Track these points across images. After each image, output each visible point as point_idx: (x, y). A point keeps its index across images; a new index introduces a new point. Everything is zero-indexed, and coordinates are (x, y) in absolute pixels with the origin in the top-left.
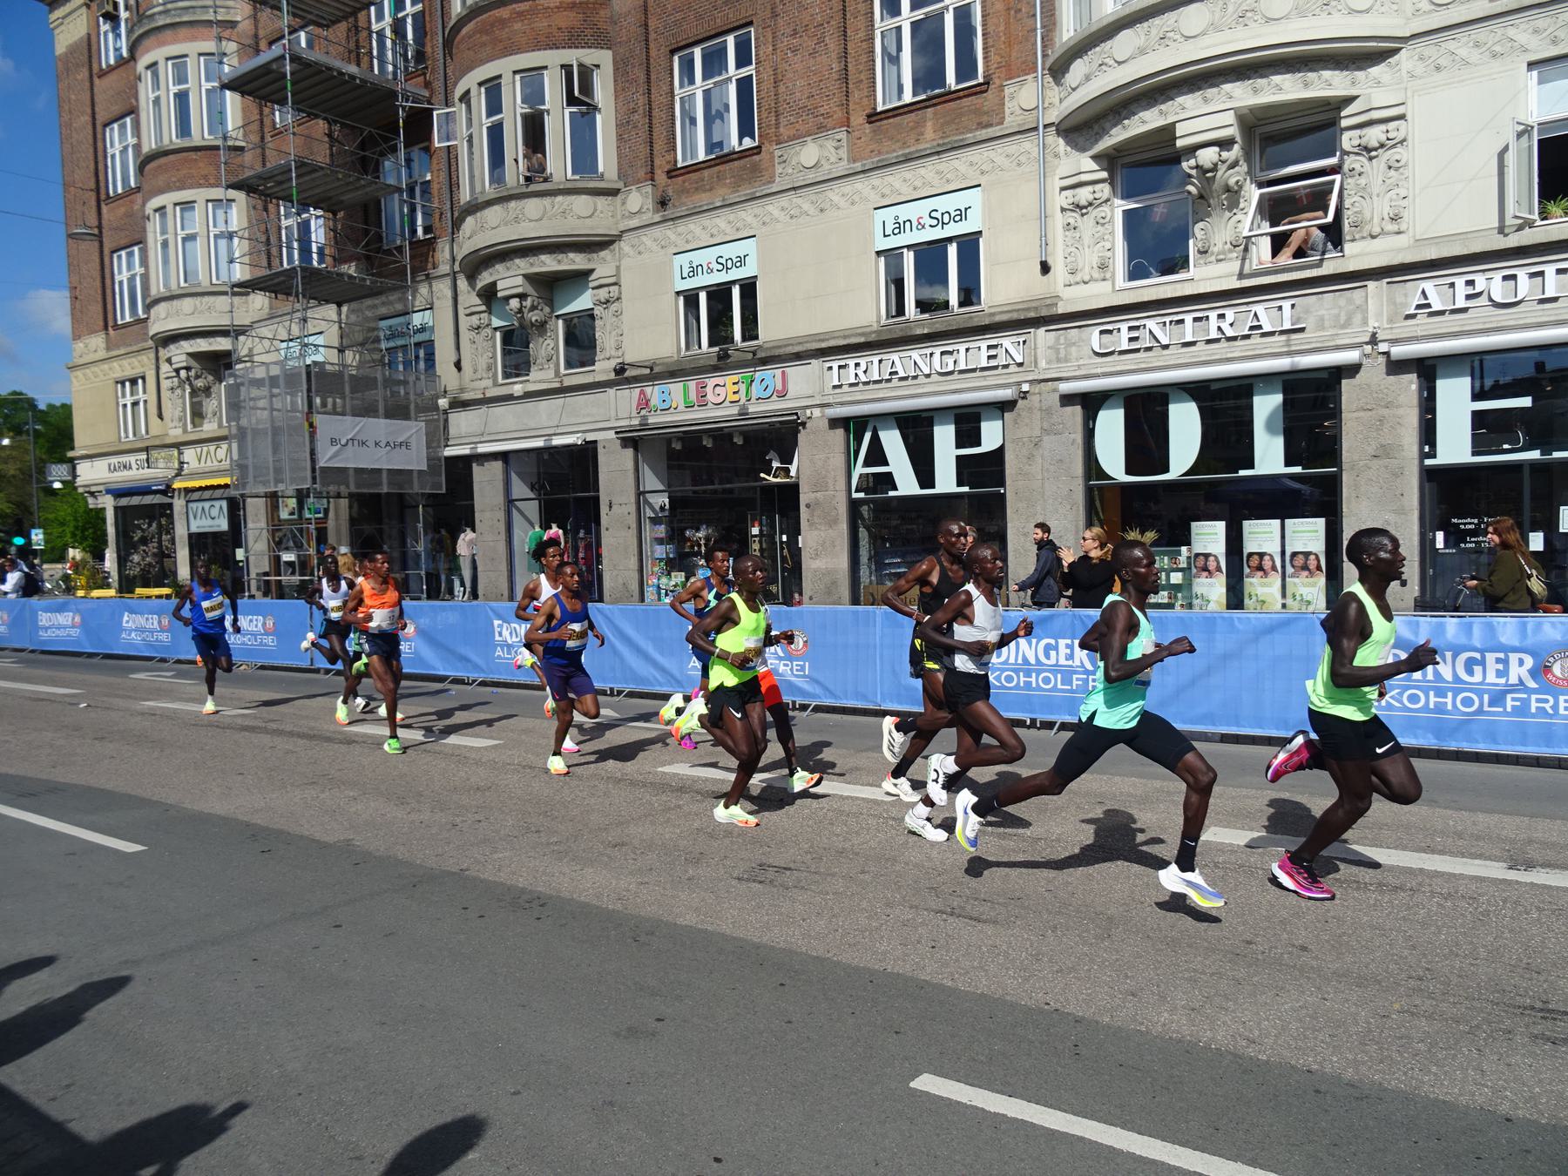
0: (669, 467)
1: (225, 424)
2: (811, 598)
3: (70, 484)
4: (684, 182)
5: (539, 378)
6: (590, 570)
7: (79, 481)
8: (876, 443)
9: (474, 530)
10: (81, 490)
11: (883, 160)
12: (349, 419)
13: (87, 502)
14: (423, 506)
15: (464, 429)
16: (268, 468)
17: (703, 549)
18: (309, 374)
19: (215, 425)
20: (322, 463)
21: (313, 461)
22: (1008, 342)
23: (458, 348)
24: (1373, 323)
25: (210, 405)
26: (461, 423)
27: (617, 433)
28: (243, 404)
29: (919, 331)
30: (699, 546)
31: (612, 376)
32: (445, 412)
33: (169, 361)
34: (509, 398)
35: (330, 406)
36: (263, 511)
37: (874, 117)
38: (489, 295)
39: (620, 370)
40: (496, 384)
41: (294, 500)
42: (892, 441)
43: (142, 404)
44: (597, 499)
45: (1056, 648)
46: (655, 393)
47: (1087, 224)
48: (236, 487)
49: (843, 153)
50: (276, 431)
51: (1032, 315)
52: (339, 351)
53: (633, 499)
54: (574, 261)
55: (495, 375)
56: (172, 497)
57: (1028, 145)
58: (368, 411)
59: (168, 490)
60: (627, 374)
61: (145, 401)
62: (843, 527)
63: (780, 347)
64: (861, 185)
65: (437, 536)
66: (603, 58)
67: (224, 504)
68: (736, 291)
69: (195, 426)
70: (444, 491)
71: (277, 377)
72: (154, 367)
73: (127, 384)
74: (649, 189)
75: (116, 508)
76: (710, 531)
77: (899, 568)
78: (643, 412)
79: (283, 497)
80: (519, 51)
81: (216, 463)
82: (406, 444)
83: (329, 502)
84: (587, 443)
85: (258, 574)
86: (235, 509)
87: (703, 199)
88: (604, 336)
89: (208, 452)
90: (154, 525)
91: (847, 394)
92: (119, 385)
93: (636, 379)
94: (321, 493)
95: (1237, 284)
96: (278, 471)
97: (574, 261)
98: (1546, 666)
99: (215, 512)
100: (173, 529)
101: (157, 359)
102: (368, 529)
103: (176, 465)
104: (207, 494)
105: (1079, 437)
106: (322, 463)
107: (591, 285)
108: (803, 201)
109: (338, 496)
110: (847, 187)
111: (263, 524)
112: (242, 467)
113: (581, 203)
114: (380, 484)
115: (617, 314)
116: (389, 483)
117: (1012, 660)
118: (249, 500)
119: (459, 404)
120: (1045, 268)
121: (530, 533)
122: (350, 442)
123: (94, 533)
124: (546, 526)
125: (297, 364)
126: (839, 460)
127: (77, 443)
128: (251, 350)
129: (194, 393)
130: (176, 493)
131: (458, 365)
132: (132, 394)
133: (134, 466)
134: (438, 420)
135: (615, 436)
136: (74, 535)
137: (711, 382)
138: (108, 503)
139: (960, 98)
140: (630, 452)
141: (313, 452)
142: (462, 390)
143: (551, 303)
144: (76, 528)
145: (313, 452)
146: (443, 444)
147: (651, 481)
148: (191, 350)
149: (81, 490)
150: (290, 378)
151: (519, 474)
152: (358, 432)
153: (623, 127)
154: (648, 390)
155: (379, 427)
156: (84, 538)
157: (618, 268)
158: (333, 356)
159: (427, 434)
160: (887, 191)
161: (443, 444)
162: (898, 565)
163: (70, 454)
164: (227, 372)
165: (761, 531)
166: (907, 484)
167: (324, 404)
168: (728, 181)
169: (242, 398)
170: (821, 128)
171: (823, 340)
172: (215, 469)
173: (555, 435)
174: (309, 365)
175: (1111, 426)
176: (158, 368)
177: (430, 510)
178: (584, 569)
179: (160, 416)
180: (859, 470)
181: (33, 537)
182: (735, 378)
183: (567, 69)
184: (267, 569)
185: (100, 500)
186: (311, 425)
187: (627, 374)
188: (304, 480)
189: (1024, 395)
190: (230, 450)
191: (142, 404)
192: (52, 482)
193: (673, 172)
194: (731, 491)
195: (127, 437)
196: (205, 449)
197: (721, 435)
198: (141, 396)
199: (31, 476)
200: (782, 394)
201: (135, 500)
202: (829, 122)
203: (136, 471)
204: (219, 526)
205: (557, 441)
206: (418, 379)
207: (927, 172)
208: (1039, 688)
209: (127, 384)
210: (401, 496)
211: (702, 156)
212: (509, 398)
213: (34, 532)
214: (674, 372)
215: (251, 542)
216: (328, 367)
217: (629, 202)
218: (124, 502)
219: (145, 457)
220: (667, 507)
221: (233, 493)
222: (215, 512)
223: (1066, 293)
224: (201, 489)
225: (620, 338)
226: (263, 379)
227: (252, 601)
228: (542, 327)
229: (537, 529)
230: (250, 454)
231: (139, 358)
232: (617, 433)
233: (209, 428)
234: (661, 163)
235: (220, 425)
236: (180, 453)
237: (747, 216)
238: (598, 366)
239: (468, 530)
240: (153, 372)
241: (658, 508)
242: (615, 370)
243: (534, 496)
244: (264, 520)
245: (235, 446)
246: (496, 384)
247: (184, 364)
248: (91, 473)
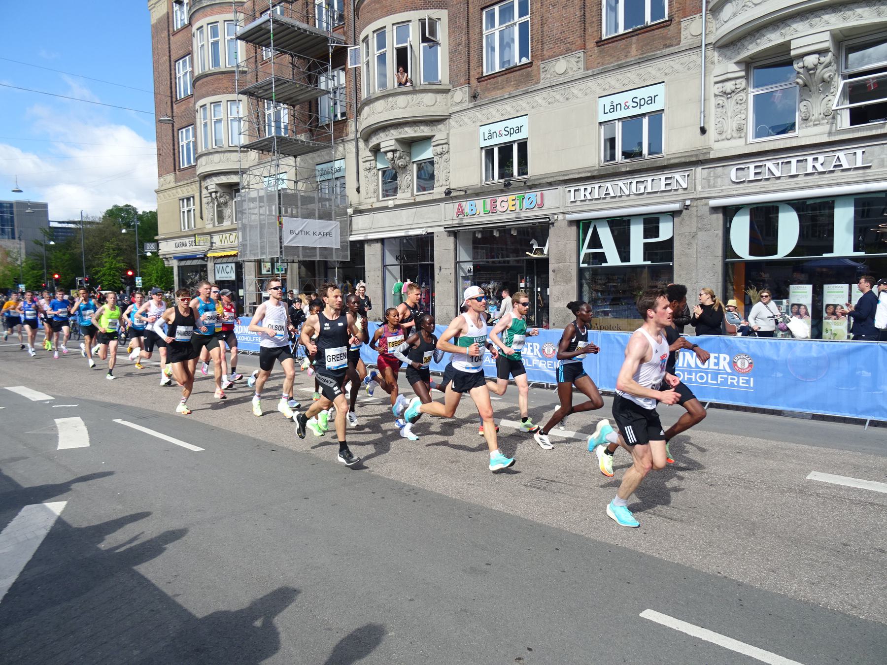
0: (474, 248)
1: (234, 222)
2: (554, 324)
3: (155, 254)
4: (487, 84)
5: (403, 197)
6: (428, 305)
7: (160, 252)
8: (595, 234)
9: (364, 282)
10: (161, 257)
11: (606, 68)
12: (300, 219)
13: (164, 263)
14: (338, 268)
15: (360, 227)
16: (257, 246)
17: (491, 294)
18: (279, 195)
19: (229, 223)
20: (285, 244)
21: (281, 242)
22: (678, 176)
23: (358, 181)
25: (227, 212)
26: (359, 222)
27: (445, 228)
28: (244, 212)
29: (623, 170)
30: (489, 293)
31: (443, 196)
32: (351, 216)
33: (207, 188)
34: (386, 208)
35: (289, 210)
36: (253, 269)
37: (600, 43)
38: (376, 150)
39: (448, 193)
40: (378, 201)
41: (270, 264)
42: (605, 235)
43: (192, 211)
44: (432, 266)
46: (467, 205)
47: (730, 105)
48: (241, 256)
49: (581, 65)
50: (262, 227)
51: (694, 159)
52: (295, 182)
53: (453, 266)
54: (424, 131)
55: (378, 196)
56: (207, 261)
57: (696, 58)
58: (309, 215)
59: (205, 258)
60: (453, 194)
61: (194, 210)
62: (574, 283)
63: (540, 179)
65: (345, 285)
66: (442, 15)
67: (233, 265)
69: (219, 224)
70: (349, 260)
71: (263, 196)
72: (199, 191)
73: (185, 200)
74: (467, 89)
75: (179, 267)
76: (496, 284)
77: (605, 308)
78: (460, 217)
79: (263, 262)
80: (396, 12)
81: (229, 243)
82: (329, 234)
83: (288, 265)
84: (428, 233)
85: (250, 304)
86: (239, 267)
87: (498, 94)
88: (440, 173)
89: (226, 237)
90: (198, 276)
91: (579, 206)
92: (181, 201)
93: (456, 197)
94: (284, 260)
95: (826, 139)
96: (262, 248)
97: (424, 131)
99: (228, 270)
100: (207, 278)
101: (200, 187)
102: (309, 280)
103: (209, 244)
104: (225, 260)
105: (720, 232)
106: (285, 244)
107: (433, 144)
108: (557, 94)
109: (293, 262)
110: (583, 85)
111: (253, 277)
112: (244, 246)
113: (428, 98)
114: (316, 256)
115: (447, 161)
116: (320, 255)
118: (246, 263)
119: (358, 212)
120: (703, 131)
121: (395, 284)
122: (300, 233)
123: (167, 279)
124: (404, 281)
125: (273, 190)
126: (573, 245)
127: (159, 233)
128: (249, 182)
129: (219, 206)
130: (209, 259)
131: (358, 190)
132: (187, 206)
133: (188, 245)
134: (347, 220)
135: (444, 230)
136: (156, 281)
137: (499, 200)
138: (175, 264)
139: (653, 30)
140: (452, 239)
141: (281, 238)
142: (360, 204)
143: (410, 154)
144: (158, 277)
145: (281, 238)
146: (349, 234)
147: (464, 256)
148: (218, 182)
149: (161, 257)
150: (270, 197)
151: (389, 251)
152: (304, 227)
153: (453, 54)
154: (463, 204)
155: (315, 224)
156: (162, 282)
157: (448, 134)
158: (292, 185)
159: (341, 228)
160: (607, 87)
161: (349, 234)
162: (605, 306)
163: (156, 238)
164: (237, 194)
165: (526, 285)
166: (613, 259)
167: (286, 212)
168: (512, 83)
169: (244, 208)
170: (568, 51)
171: (566, 175)
172: (229, 246)
173: (411, 229)
174: (280, 190)
175: (741, 228)
176: (201, 192)
177: (341, 270)
178: (424, 304)
179: (202, 218)
180: (585, 250)
181: (137, 281)
182: (513, 197)
183: (423, 21)
184: (255, 301)
185: (171, 262)
186: (280, 223)
187: (452, 195)
188: (276, 253)
189: (687, 207)
190: (237, 237)
191: (192, 211)
192: (146, 252)
193: (481, 79)
194: (508, 262)
195: (185, 229)
196: (224, 235)
197: (504, 230)
198: (192, 207)
199: (135, 249)
200: (541, 206)
201: (189, 263)
202: (574, 47)
203: (189, 248)
204: (231, 277)
205: (412, 233)
206: (336, 198)
207: (632, 75)
209: (185, 200)
210: (326, 262)
212: (386, 208)
213: (137, 278)
214: (478, 193)
215: (247, 288)
216: (289, 191)
217: (455, 96)
218: (183, 263)
219: (194, 239)
220: (472, 270)
221: (239, 259)
222: (228, 270)
223: (716, 146)
224: (222, 257)
225: (448, 174)
226: (256, 198)
227: (247, 318)
228: (404, 168)
229: (399, 281)
230: (248, 238)
231: (191, 186)
232: (445, 228)
233: (227, 224)
234: (474, 74)
235: (232, 223)
236: (211, 238)
237: (523, 103)
238: (435, 190)
239: (361, 281)
240: (198, 194)
241: (467, 271)
242: (445, 193)
243: (397, 264)
244: (254, 274)
245: (240, 234)
246: (378, 201)
247: (214, 190)
248: (166, 248)
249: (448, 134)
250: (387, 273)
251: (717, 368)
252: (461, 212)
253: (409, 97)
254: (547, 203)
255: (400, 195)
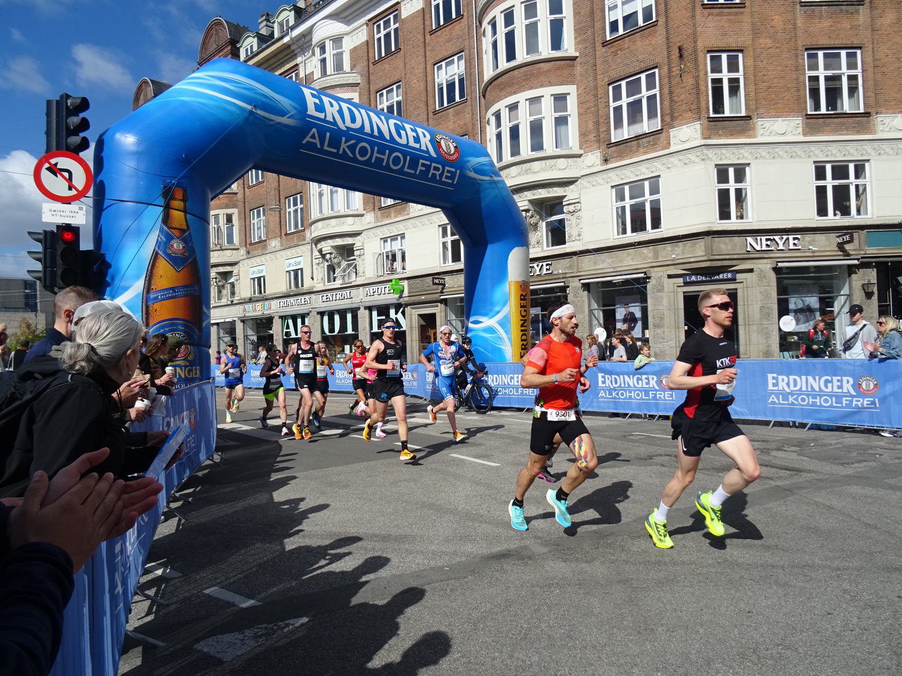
8: (288, 322)
22: (307, 297)
24: (362, 297)
37: (286, 234)
42: (290, 322)
45: (513, 378)
47: (319, 268)
64: (282, 253)
68: (262, 279)
95: (340, 286)
98: (859, 384)
105: (319, 323)
113: (228, 253)
115: (239, 283)
117: (501, 384)
137: (257, 304)
143: (226, 280)
157: (239, 271)
175: (326, 318)
182: (261, 304)
189: (311, 312)
193: (251, 244)
202: (277, 235)
205: (227, 320)
208: (509, 395)
211: (257, 241)
214: (250, 300)
223: (317, 285)
234: (248, 242)
237: (263, 258)
249: (239, 271)
250: (221, 341)
251: (648, 386)
252: (245, 310)
253: (219, 252)
254: (273, 307)
255: (223, 300)
